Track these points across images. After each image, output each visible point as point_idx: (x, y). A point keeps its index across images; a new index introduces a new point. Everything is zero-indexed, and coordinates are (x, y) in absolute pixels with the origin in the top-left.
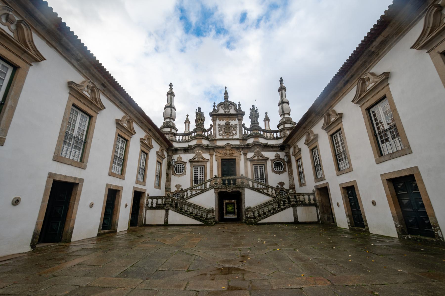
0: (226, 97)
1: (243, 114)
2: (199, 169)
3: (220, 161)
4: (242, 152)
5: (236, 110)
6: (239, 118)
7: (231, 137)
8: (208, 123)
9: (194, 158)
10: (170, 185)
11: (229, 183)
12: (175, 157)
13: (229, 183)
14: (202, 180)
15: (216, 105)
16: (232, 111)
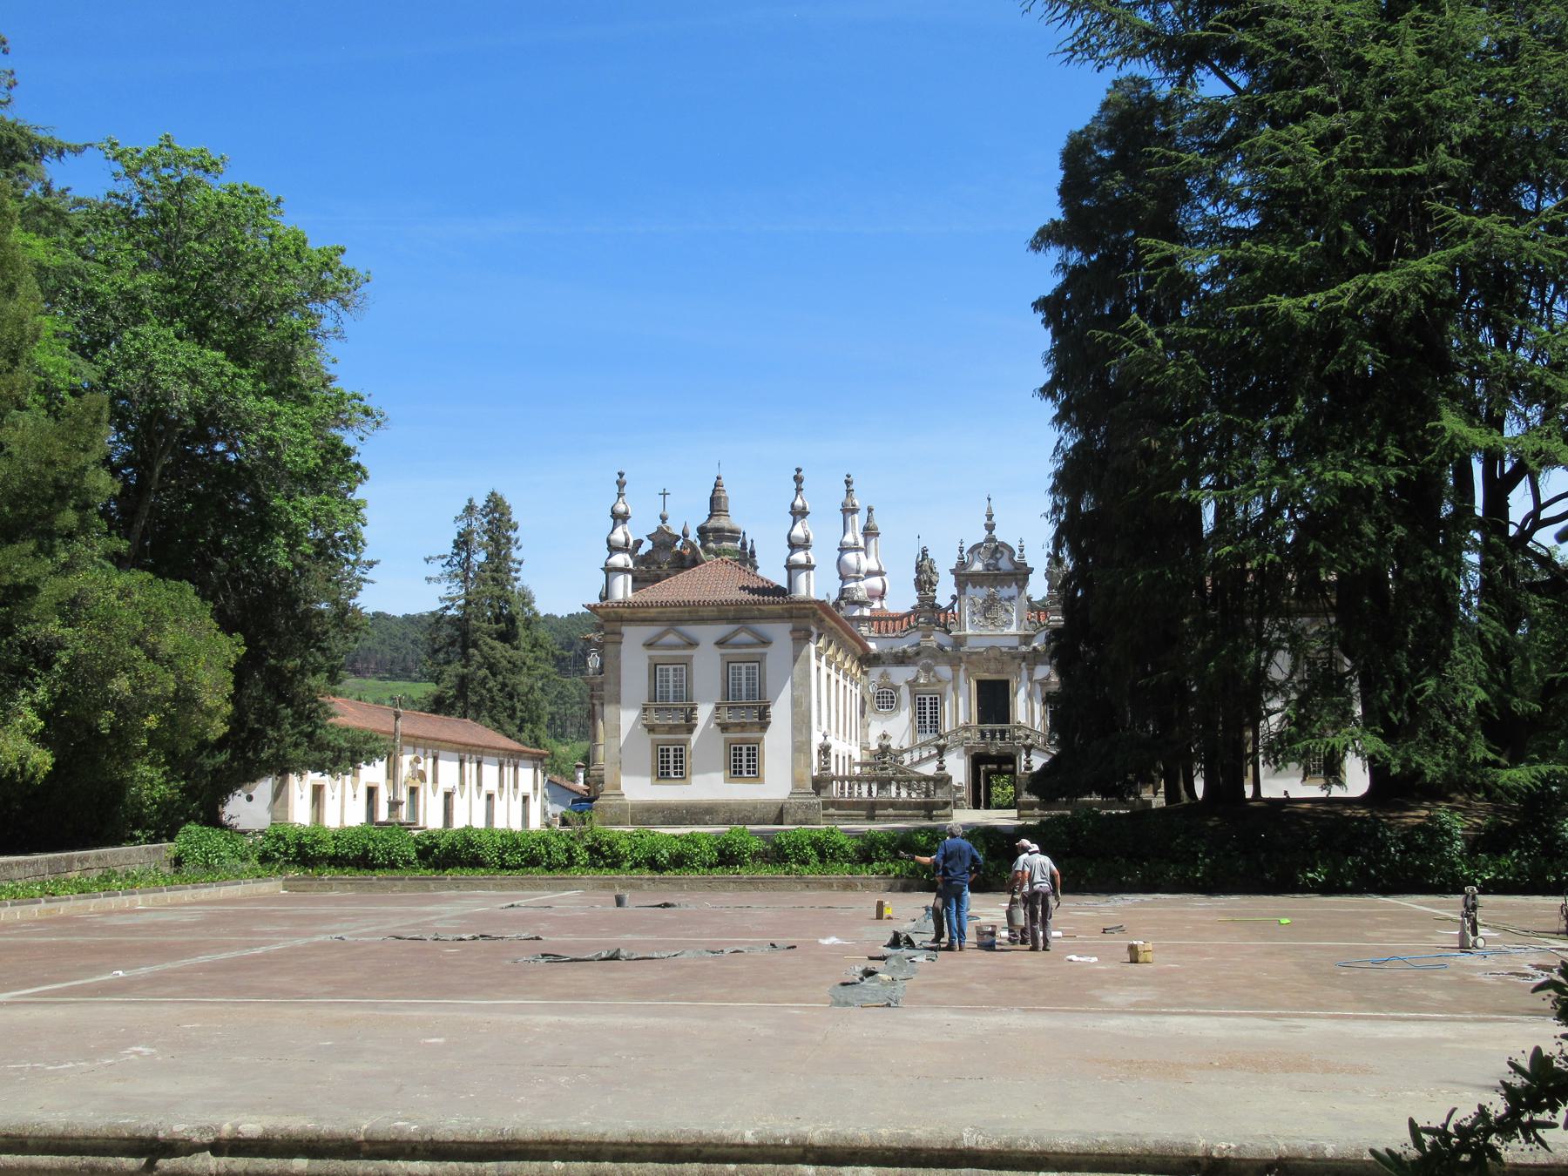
0: (990, 527)
1: (1031, 570)
2: (928, 702)
3: (974, 685)
4: (1023, 665)
5: (1011, 559)
6: (1021, 583)
7: (998, 632)
8: (945, 592)
9: (917, 678)
10: (867, 736)
11: (993, 737)
12: (876, 672)
13: (993, 737)
14: (936, 724)
15: (967, 548)
16: (1004, 564)
